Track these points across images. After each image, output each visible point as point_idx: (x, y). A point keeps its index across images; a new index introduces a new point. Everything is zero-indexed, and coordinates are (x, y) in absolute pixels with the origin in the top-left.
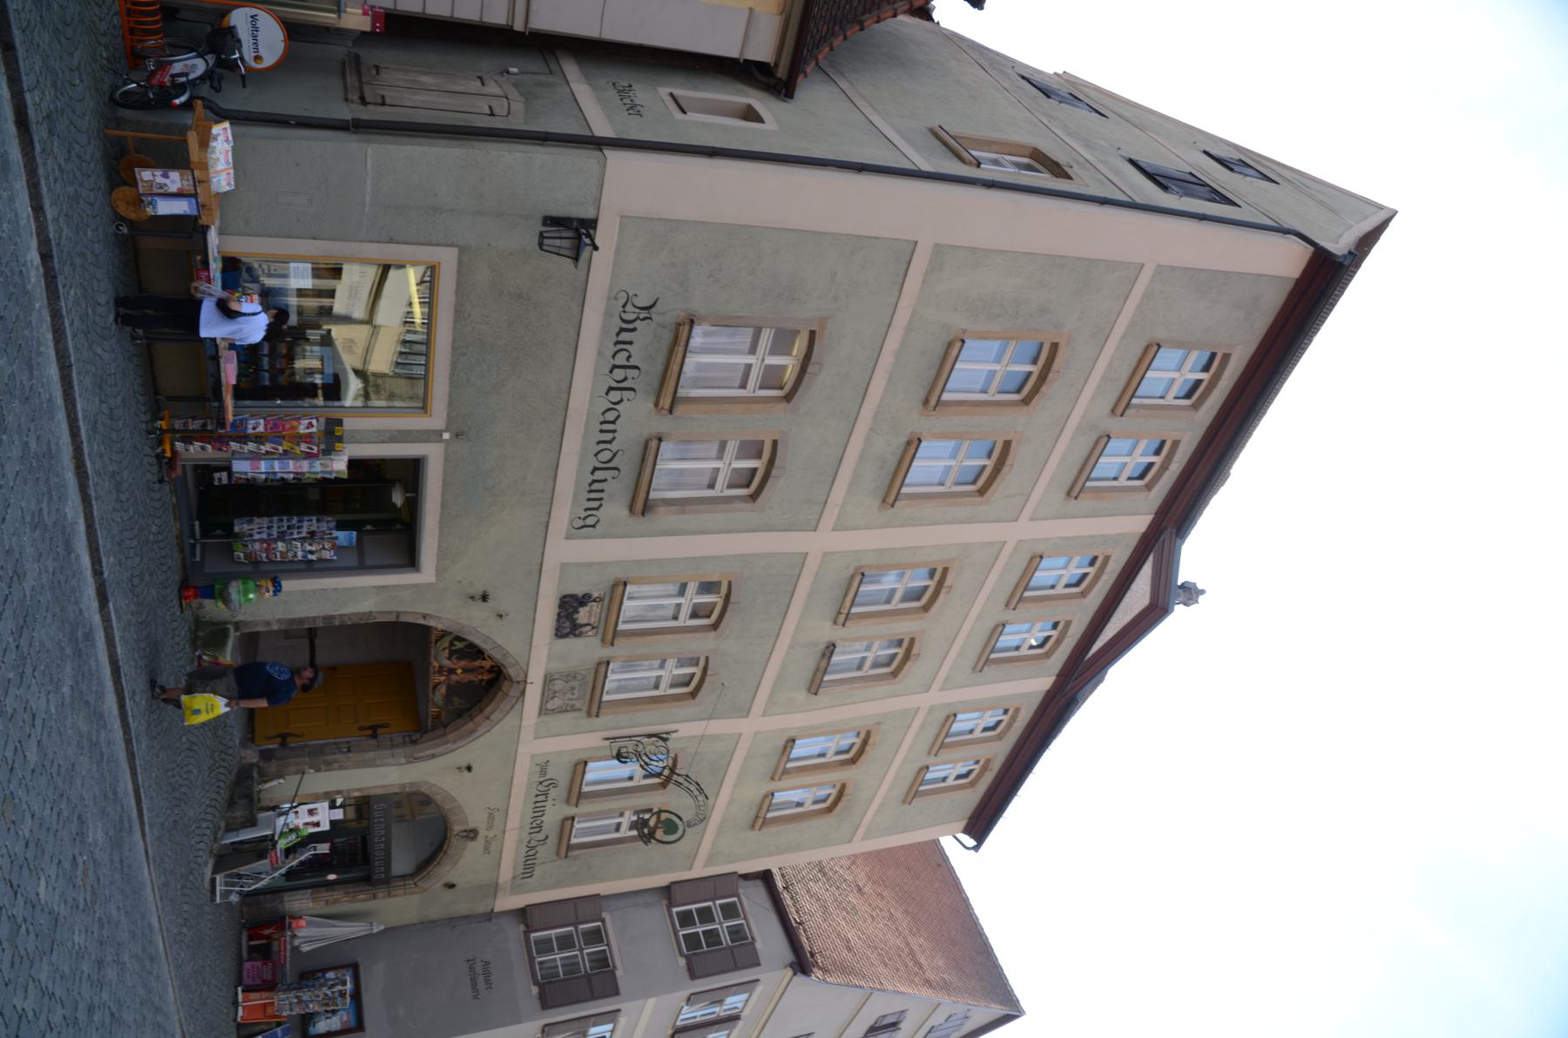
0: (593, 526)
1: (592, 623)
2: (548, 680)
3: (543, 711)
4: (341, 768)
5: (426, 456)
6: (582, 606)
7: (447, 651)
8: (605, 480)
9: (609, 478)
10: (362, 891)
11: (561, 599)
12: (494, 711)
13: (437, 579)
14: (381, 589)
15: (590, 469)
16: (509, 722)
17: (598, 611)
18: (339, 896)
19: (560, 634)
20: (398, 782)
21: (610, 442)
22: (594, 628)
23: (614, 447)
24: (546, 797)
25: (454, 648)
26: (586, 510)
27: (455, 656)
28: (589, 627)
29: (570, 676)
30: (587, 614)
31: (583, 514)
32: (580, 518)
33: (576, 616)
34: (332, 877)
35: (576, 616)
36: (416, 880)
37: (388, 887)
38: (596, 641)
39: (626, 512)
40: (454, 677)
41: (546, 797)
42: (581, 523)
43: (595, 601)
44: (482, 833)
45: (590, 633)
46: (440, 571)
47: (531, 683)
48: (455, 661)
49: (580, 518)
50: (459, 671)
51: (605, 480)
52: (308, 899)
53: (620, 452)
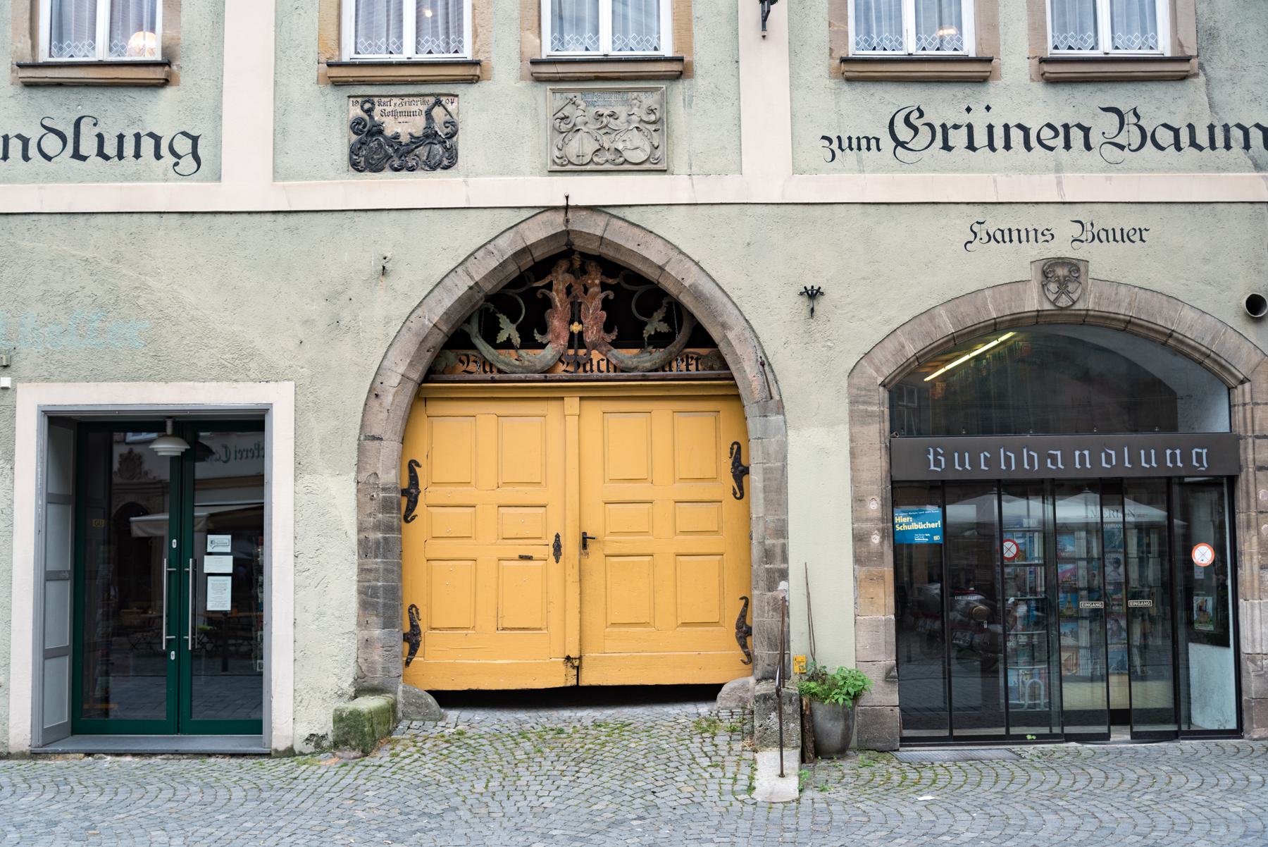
0: (195, 140)
1: (424, 108)
2: (563, 167)
3: (654, 166)
4: (781, 531)
5: (39, 406)
6: (381, 132)
7: (523, 352)
8: (100, 137)
9: (97, 130)
10: (1248, 493)
11: (358, 170)
12: (645, 259)
13: (289, 380)
14: (300, 467)
15: (76, 162)
16: (675, 228)
17: (395, 100)
18: (1255, 539)
19: (449, 160)
20: (844, 431)
21: (25, 142)
22: (438, 103)
23: (33, 133)
24: (956, 127)
25: (516, 340)
26: (158, 156)
27: (538, 337)
28: (438, 113)
29: (564, 126)
30: (401, 119)
31: (168, 159)
32: (176, 164)
33: (405, 139)
34: (1203, 555)
35: (405, 139)
36: (1233, 382)
37: (1245, 438)
38: (468, 94)
39: (168, 92)
40: (590, 337)
41: (956, 127)
42: (188, 163)
43: (369, 111)
44: (1061, 248)
45: (450, 107)
46: (270, 375)
47: (567, 197)
48: (550, 336)
49: (176, 164)
50: (576, 328)
51: (100, 136)
52: (1252, 606)
53: (46, 122)
